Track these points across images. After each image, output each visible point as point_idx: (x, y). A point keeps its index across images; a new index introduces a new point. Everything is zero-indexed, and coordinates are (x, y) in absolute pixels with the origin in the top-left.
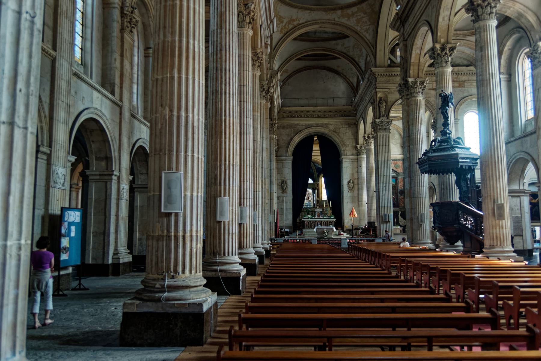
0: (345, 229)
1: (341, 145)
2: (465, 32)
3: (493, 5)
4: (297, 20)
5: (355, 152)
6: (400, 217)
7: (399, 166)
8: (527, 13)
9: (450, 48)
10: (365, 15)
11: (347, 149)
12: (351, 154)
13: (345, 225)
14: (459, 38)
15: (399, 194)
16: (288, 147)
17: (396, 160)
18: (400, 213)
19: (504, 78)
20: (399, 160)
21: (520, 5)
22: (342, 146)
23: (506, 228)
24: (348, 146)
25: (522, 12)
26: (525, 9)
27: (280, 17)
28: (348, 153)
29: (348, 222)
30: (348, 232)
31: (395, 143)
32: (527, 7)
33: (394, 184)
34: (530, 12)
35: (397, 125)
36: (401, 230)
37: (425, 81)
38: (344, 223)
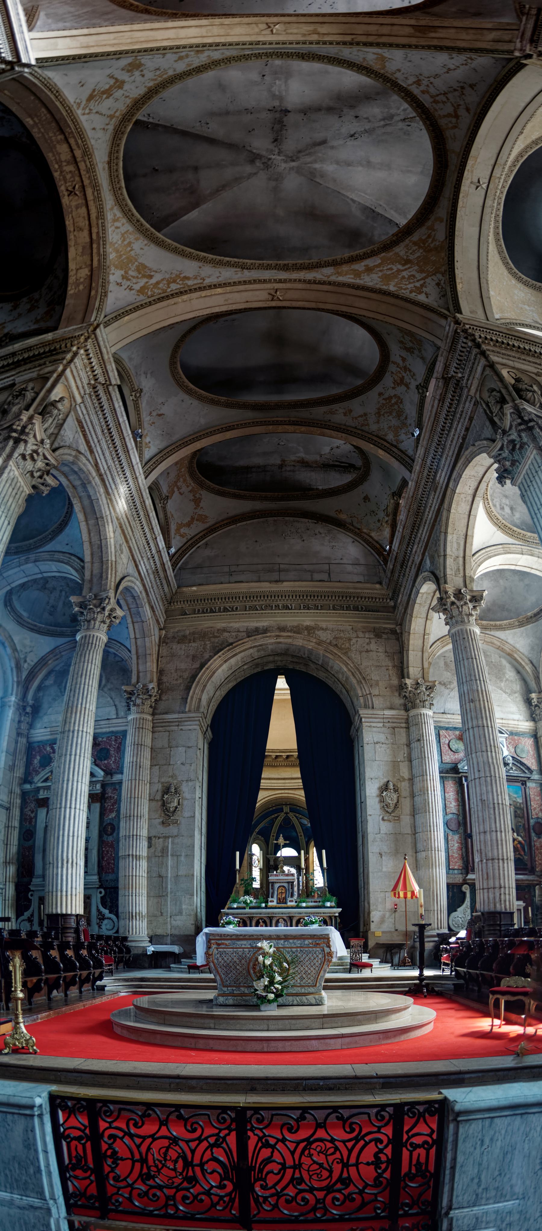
0: (371, 944)
1: (354, 681)
4: (196, 278)
5: (398, 701)
10: (409, 266)
11: (375, 691)
12: (388, 704)
13: (373, 927)
15: (533, 834)
16: (188, 688)
22: (359, 682)
24: (377, 685)
27: (144, 266)
28: (377, 702)
29: (382, 921)
30: (381, 951)
33: (520, 800)
38: (367, 923)
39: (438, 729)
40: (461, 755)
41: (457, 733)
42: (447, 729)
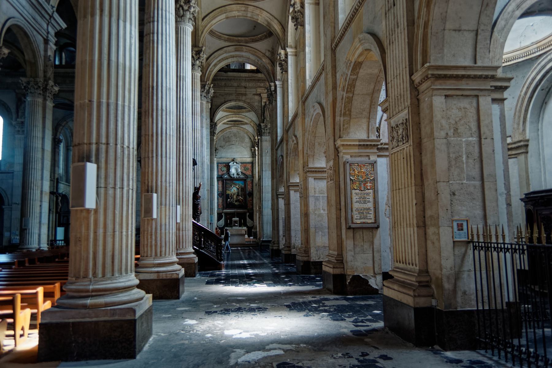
2: (246, 38)
3: (186, 8)
6: (247, 218)
7: (248, 169)
8: (273, 22)
9: (197, 51)
14: (241, 44)
17: (246, 163)
18: (248, 214)
19: (280, 85)
20: (248, 163)
21: (267, 13)
23: (183, 231)
25: (269, 20)
26: (271, 17)
31: (245, 147)
32: (273, 16)
34: (276, 21)
35: (247, 128)
36: (246, 231)
37: (206, 84)
39: (218, 163)
40: (225, 172)
41: (224, 164)
42: (221, 163)
